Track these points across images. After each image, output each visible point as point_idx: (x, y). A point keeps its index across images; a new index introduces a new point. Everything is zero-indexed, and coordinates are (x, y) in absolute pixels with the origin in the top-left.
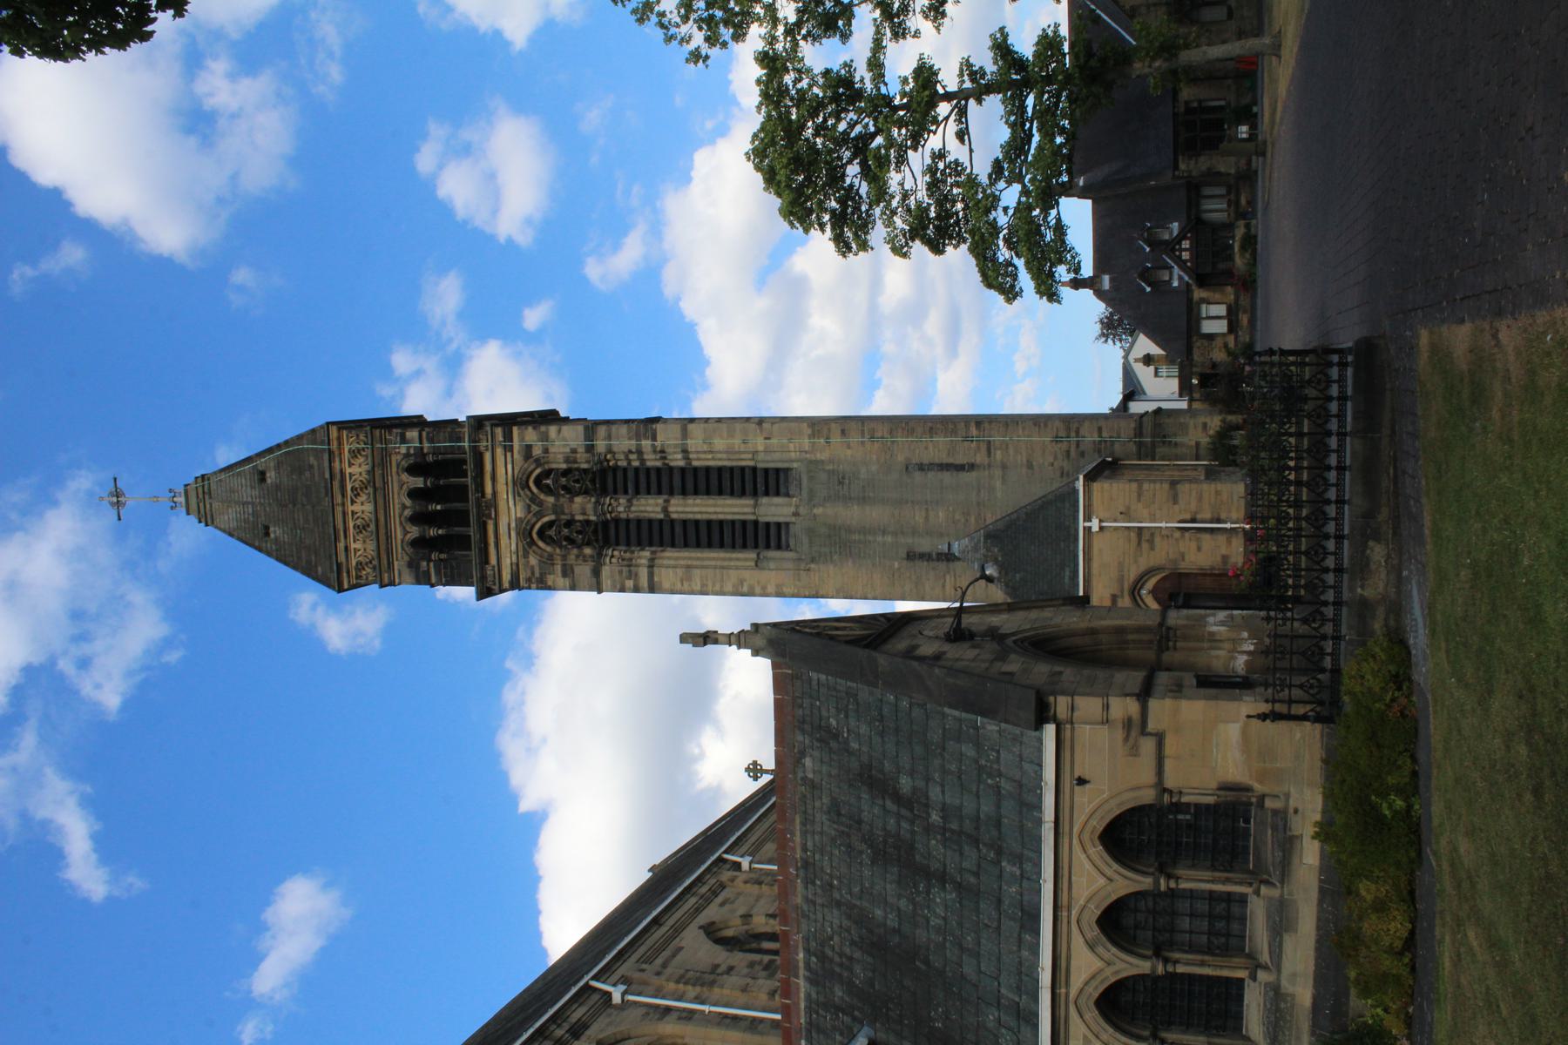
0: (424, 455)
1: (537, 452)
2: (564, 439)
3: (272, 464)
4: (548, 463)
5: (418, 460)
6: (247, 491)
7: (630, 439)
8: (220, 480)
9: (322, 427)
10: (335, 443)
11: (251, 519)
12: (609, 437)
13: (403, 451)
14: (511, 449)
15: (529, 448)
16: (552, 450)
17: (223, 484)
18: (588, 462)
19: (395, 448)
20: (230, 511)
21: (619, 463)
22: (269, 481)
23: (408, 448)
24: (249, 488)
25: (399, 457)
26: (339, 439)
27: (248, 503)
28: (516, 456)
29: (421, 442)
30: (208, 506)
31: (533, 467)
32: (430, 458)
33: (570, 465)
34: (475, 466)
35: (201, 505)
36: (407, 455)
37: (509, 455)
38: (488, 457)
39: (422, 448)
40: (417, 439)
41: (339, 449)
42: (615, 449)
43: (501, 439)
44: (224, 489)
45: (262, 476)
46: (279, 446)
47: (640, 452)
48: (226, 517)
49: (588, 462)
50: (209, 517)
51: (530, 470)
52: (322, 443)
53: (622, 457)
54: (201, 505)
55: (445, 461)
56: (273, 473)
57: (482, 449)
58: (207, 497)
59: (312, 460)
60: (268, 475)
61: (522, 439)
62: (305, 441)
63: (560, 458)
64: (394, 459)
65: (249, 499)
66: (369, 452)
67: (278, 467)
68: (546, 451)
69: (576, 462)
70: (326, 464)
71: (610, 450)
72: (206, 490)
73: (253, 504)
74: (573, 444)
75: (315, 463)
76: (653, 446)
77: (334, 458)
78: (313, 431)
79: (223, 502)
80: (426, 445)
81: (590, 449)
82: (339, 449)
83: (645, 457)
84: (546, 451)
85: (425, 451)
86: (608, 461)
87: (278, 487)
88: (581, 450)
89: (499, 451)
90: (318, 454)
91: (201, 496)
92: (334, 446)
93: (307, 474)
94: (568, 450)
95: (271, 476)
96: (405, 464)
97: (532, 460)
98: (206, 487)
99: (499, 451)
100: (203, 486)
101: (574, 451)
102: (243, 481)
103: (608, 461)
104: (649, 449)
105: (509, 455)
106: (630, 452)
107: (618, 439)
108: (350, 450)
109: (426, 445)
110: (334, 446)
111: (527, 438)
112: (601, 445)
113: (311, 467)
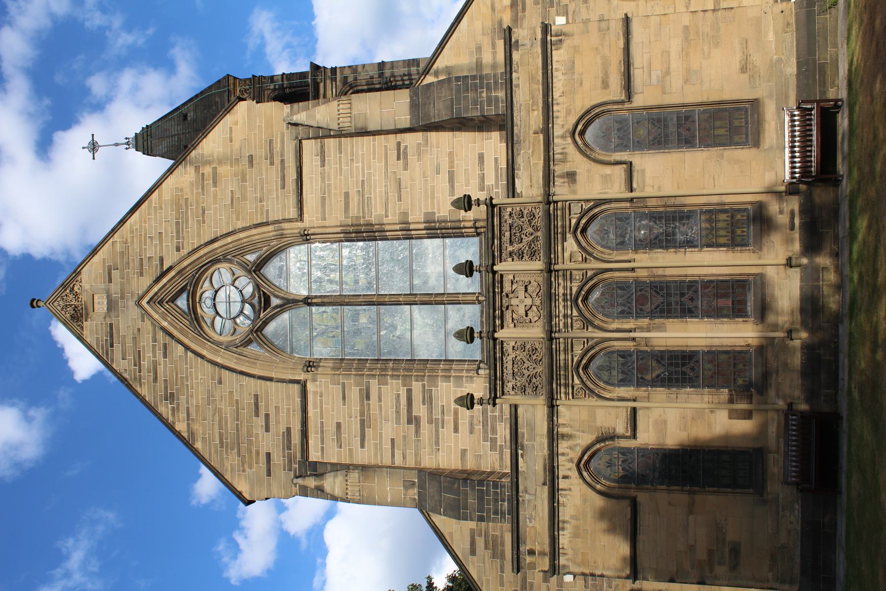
0: (284, 89)
1: (350, 79)
2: (367, 71)
3: (192, 108)
4: (356, 86)
5: (280, 92)
6: (174, 128)
7: (404, 67)
8: (158, 126)
9: (224, 78)
10: (232, 86)
11: (176, 144)
12: (392, 68)
13: (272, 87)
14: (336, 81)
15: (346, 78)
16: (358, 78)
17: (160, 127)
18: (380, 83)
19: (267, 86)
20: (163, 142)
21: (398, 83)
22: (189, 118)
23: (275, 85)
24: (176, 126)
25: (269, 92)
26: (234, 84)
27: (175, 135)
28: (338, 83)
29: (283, 81)
30: (149, 143)
31: (348, 89)
32: (287, 91)
33: (369, 87)
34: (315, 90)
35: (145, 143)
36: (275, 89)
37: (334, 83)
38: (322, 85)
39: (283, 84)
40: (280, 80)
41: (234, 89)
42: (396, 74)
43: (330, 75)
44: (160, 131)
45: (185, 117)
46: (197, 96)
47: (410, 75)
48: (161, 147)
49: (380, 83)
50: (149, 149)
51: (346, 90)
52: (225, 87)
53: (399, 79)
54: (145, 143)
55: (295, 92)
56: (192, 113)
57: (319, 80)
58: (149, 138)
59: (218, 99)
60: (189, 115)
61: (342, 73)
62: (213, 89)
63: (364, 82)
64: (266, 92)
65: (176, 133)
66: (252, 89)
67: (195, 110)
68: (356, 79)
69: (373, 84)
70: (226, 98)
71: (393, 76)
72: (149, 134)
73: (178, 135)
74: (371, 73)
75: (219, 100)
76: (418, 70)
77: (231, 94)
78: (219, 81)
79: (159, 139)
80: (285, 82)
81: (381, 75)
82: (234, 89)
83: (413, 77)
84: (356, 79)
85: (285, 86)
86: (391, 82)
87: (195, 120)
88: (376, 76)
89: (328, 82)
90: (221, 95)
91: (145, 138)
92: (232, 87)
93: (214, 108)
94: (369, 77)
95: (191, 116)
96: (272, 95)
97: (347, 85)
98: (149, 132)
99: (328, 82)
100: (147, 131)
101: (372, 78)
102: (173, 122)
103: (391, 82)
104: (415, 72)
105: (334, 83)
106: (405, 75)
107: (397, 68)
108: (240, 90)
109: (285, 82)
110: (232, 87)
111: (344, 73)
112: (387, 73)
113: (216, 103)
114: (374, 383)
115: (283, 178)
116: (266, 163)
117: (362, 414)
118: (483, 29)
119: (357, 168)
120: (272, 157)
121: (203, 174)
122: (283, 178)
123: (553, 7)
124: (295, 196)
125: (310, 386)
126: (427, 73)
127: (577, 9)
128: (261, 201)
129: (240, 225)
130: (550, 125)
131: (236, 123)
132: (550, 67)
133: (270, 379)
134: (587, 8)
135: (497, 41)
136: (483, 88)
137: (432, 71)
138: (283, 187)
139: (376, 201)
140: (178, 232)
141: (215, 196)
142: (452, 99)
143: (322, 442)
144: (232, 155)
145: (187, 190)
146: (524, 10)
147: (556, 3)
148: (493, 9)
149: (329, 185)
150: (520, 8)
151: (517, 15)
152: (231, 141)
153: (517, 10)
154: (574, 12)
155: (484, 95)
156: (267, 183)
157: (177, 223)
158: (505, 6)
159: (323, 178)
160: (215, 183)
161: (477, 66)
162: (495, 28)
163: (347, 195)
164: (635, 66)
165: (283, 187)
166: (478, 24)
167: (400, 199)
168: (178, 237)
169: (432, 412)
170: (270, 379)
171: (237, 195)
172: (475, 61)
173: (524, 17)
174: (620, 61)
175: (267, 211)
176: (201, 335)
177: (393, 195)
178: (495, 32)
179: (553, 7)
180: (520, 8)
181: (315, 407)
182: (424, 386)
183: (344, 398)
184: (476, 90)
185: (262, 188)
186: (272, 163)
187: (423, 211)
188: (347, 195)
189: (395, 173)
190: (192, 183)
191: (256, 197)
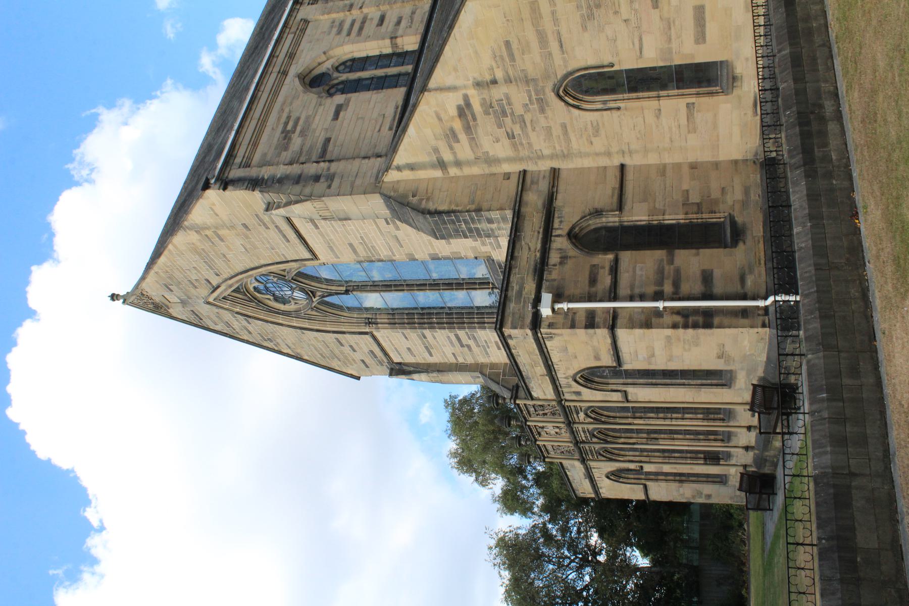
114: (427, 332)
115: (284, 236)
116: (262, 229)
117: (424, 344)
118: (434, 135)
119: (352, 230)
120: (265, 224)
121: (207, 236)
122: (284, 236)
123: (507, 117)
124: (303, 246)
125: (375, 333)
126: (390, 168)
127: (535, 119)
128: (273, 249)
129: (263, 262)
130: (554, 373)
131: (214, 204)
132: (545, 350)
133: (343, 333)
134: (546, 118)
135: (453, 144)
136: (460, 222)
137: (392, 167)
138: (288, 241)
139: (379, 247)
140: (210, 266)
141: (228, 247)
142: (433, 229)
143: (400, 355)
144: (224, 222)
145: (198, 244)
146: (475, 119)
147: (510, 114)
148: (440, 119)
149: (331, 240)
150: (470, 117)
151: (468, 123)
152: (217, 215)
153: (467, 120)
154: (532, 121)
155: (464, 226)
156: (271, 239)
157: (205, 262)
158: (453, 117)
159: (322, 235)
160: (222, 240)
161: (439, 163)
162: (447, 134)
163: (351, 245)
164: (623, 352)
165: (288, 241)
166: (428, 132)
167: (402, 246)
168: (212, 269)
169: (477, 342)
170: (343, 333)
171: (248, 247)
172: (435, 159)
173: (476, 126)
174: (609, 349)
175: (283, 255)
176: (270, 311)
177: (393, 243)
178: (449, 137)
179: (507, 117)
180: (470, 117)
181: (385, 341)
182: (467, 333)
183: (406, 338)
184: (455, 223)
185: (269, 242)
186: (267, 228)
187: (426, 253)
188: (351, 245)
189: (389, 232)
190: (200, 240)
191: (267, 248)
